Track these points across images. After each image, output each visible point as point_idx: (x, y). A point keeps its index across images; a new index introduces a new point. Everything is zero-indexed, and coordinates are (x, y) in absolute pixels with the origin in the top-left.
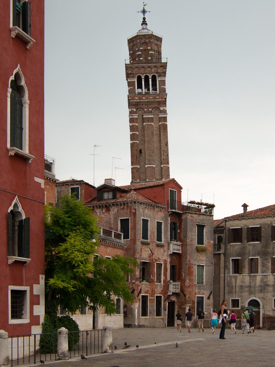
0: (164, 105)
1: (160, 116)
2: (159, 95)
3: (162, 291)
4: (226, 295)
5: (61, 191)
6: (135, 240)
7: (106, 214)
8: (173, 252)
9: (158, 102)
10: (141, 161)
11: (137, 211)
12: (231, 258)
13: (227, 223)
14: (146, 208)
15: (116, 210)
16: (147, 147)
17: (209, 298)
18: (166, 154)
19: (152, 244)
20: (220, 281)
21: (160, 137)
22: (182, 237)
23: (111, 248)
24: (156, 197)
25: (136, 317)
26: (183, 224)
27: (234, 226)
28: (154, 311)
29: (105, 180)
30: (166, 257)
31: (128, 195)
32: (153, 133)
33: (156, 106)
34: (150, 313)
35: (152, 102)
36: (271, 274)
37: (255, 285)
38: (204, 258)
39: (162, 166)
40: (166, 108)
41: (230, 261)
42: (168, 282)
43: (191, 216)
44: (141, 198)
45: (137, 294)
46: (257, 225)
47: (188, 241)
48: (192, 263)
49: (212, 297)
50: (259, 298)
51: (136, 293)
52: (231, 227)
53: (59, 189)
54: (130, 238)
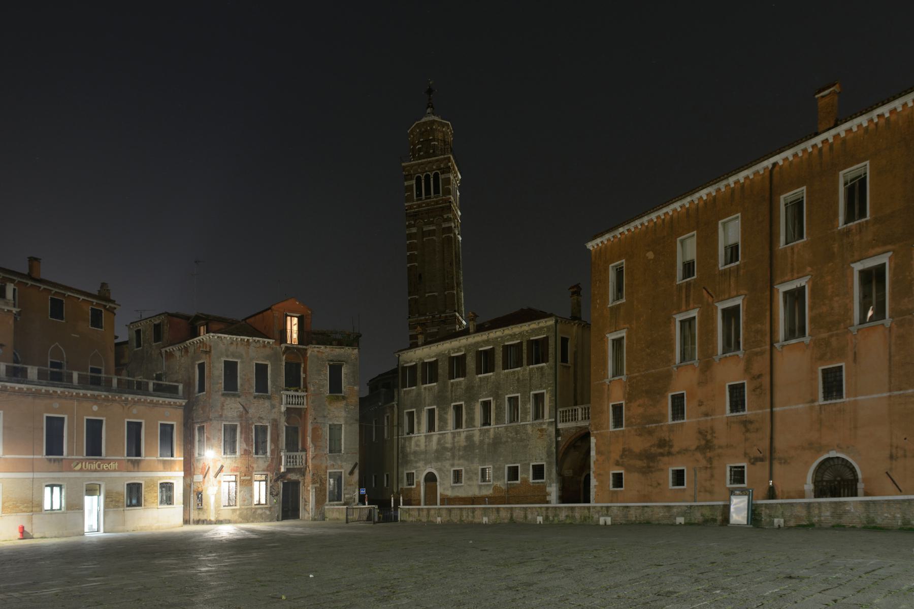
1: (443, 226)
27: (408, 363)
46: (432, 357)
52: (405, 364)
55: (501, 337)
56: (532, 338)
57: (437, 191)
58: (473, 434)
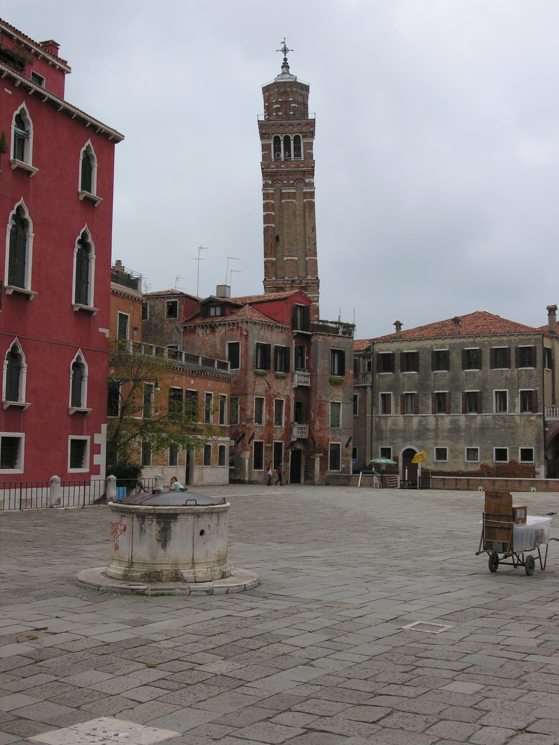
0: (311, 176)
1: (305, 190)
2: (304, 163)
3: (282, 436)
4: (374, 443)
5: (154, 306)
6: (247, 370)
7: (211, 336)
8: (298, 386)
9: (303, 172)
10: (278, 252)
11: (249, 333)
12: (380, 393)
13: (375, 346)
14: (261, 328)
15: (223, 331)
16: (287, 232)
17: (347, 446)
18: (313, 242)
20: (366, 422)
21: (305, 219)
22: (311, 366)
23: (212, 382)
24: (277, 314)
25: (247, 470)
26: (312, 348)
27: (383, 351)
29: (218, 286)
30: (288, 392)
31: (241, 312)
32: (295, 213)
33: (299, 177)
35: (294, 172)
36: (432, 415)
39: (307, 259)
40: (314, 180)
41: (378, 397)
42: (292, 424)
43: (323, 339)
44: (257, 316)
45: (248, 441)
46: (413, 349)
47: (318, 370)
48: (323, 399)
49: (351, 444)
50: (416, 446)
51: (247, 438)
52: (380, 351)
53: (152, 303)
54: (240, 367)
55: (489, 342)
56: (519, 346)
57: (298, 155)
58: (458, 419)
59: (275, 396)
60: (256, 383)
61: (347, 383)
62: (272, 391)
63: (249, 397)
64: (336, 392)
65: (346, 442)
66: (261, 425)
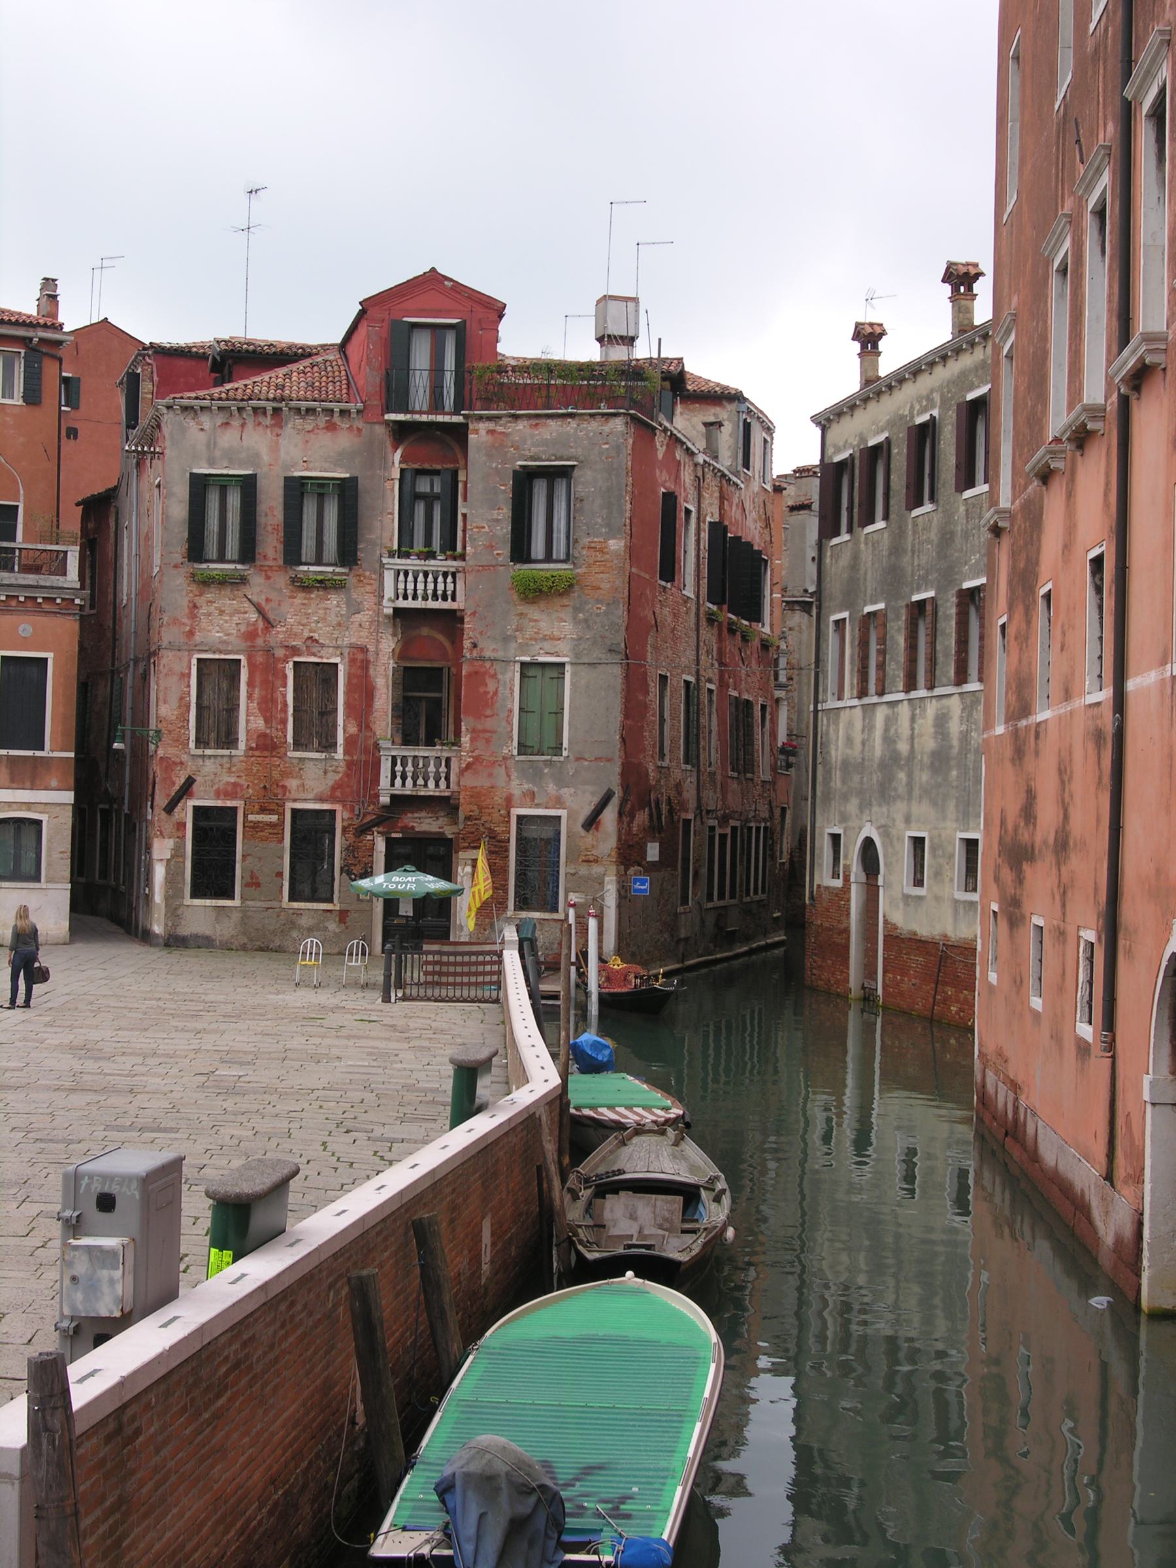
3: (333, 789)
8: (395, 609)
17: (592, 822)
19: (268, 578)
25: (158, 898)
28: (280, 874)
30: (364, 633)
34: (253, 883)
37: (873, 755)
38: (567, 628)
43: (491, 432)
48: (488, 654)
49: (609, 816)
59: (295, 651)
60: (203, 611)
61: (599, 588)
62: (278, 635)
63: (167, 659)
64: (542, 624)
65: (586, 811)
66: (226, 752)
